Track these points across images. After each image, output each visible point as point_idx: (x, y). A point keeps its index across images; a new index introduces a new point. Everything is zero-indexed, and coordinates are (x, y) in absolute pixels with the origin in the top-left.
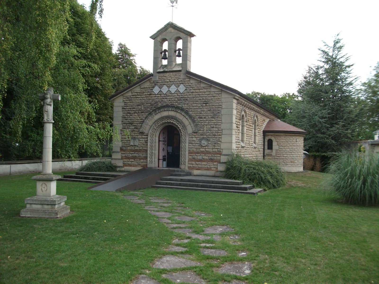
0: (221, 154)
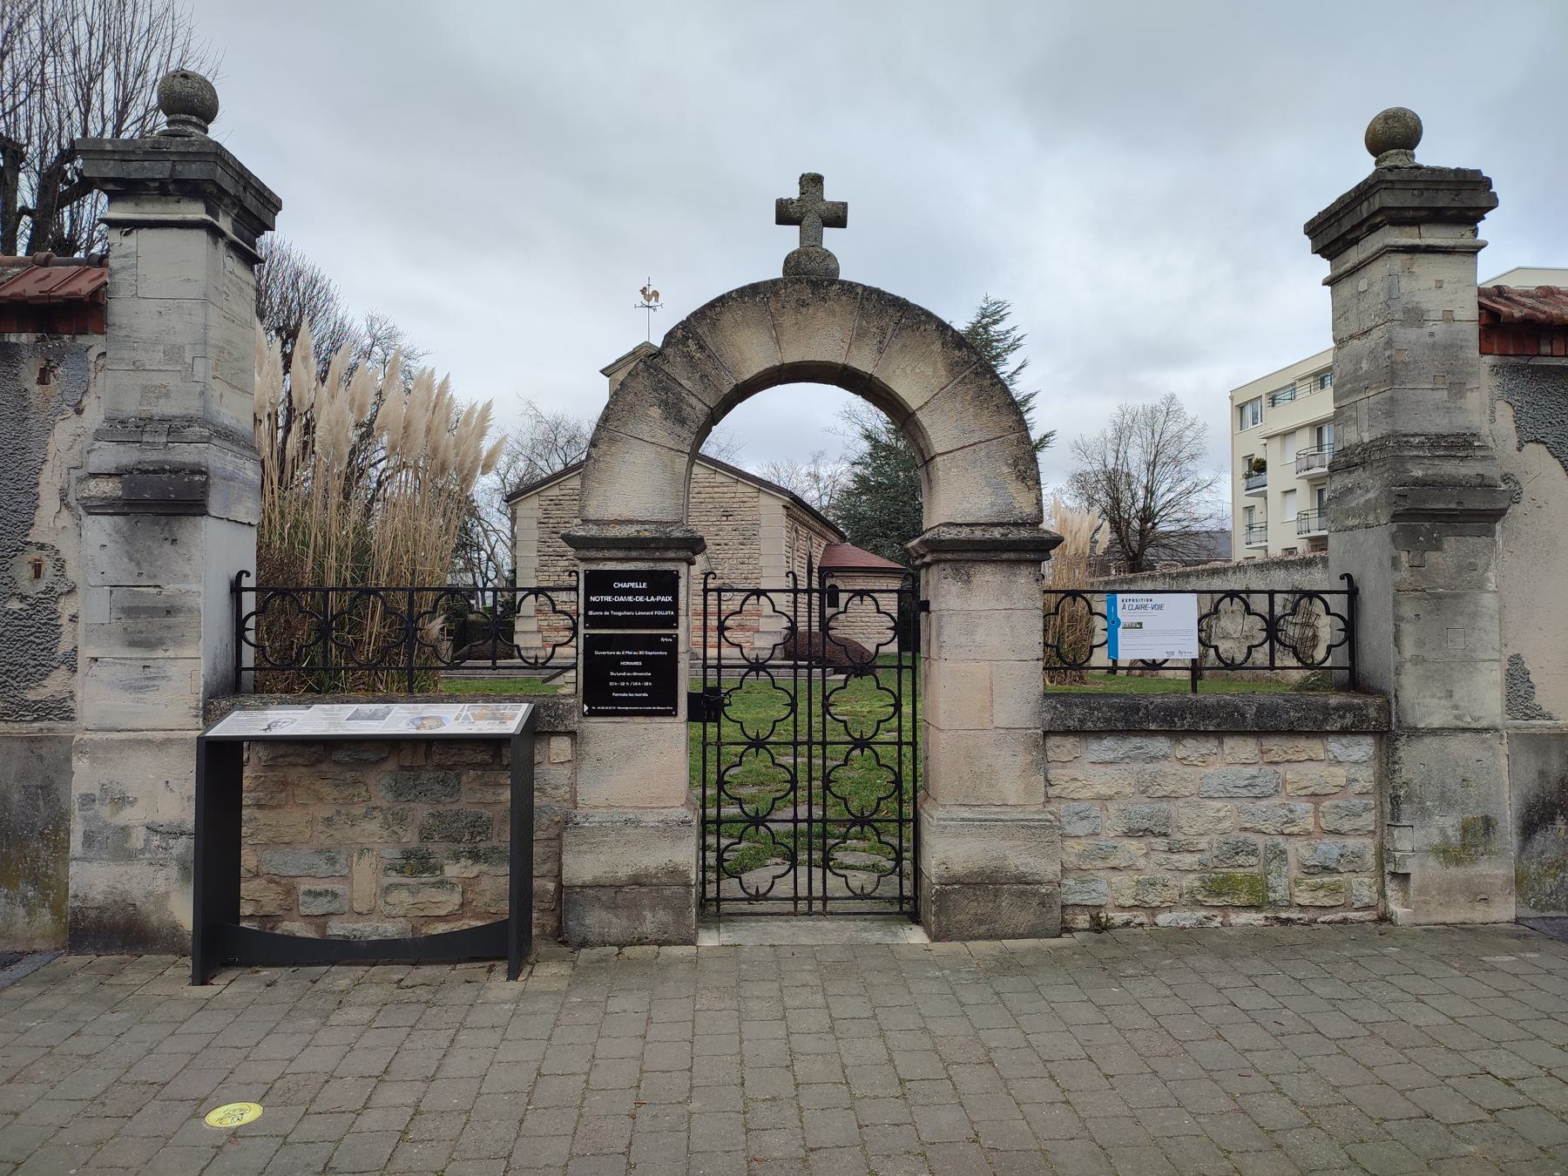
0: (759, 616)
